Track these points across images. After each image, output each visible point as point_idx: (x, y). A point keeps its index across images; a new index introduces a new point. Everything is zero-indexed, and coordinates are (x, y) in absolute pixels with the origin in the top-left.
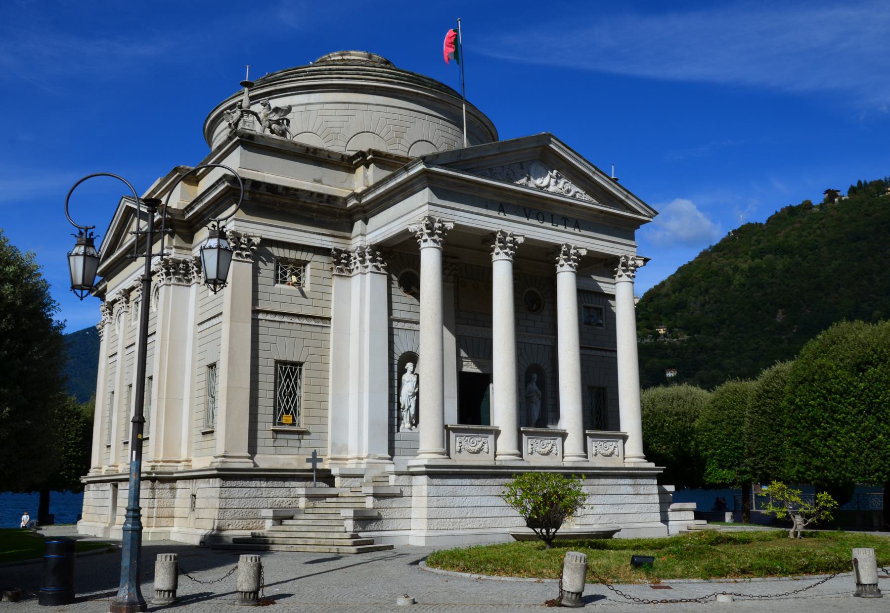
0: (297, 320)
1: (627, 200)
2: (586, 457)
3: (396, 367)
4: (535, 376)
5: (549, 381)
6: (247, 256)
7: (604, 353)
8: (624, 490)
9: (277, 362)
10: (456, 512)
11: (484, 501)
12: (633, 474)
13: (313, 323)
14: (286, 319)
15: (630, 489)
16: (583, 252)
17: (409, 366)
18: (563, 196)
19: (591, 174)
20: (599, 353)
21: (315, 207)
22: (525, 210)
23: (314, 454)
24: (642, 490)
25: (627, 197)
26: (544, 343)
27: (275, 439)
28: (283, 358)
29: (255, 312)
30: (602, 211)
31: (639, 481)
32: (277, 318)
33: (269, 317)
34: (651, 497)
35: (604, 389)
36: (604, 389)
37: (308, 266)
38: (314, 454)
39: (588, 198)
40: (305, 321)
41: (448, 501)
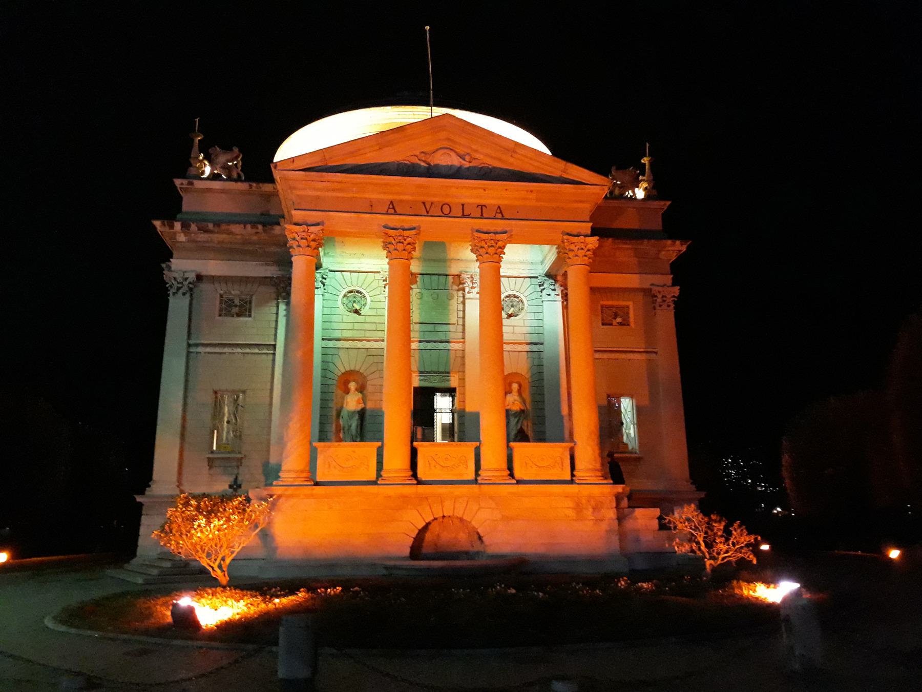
0: (239, 350)
4: (515, 386)
6: (184, 294)
13: (257, 351)
14: (226, 350)
17: (352, 386)
21: (255, 238)
22: (424, 203)
23: (236, 479)
27: (211, 467)
29: (189, 345)
32: (217, 350)
33: (208, 349)
37: (254, 297)
38: (236, 479)
40: (248, 350)
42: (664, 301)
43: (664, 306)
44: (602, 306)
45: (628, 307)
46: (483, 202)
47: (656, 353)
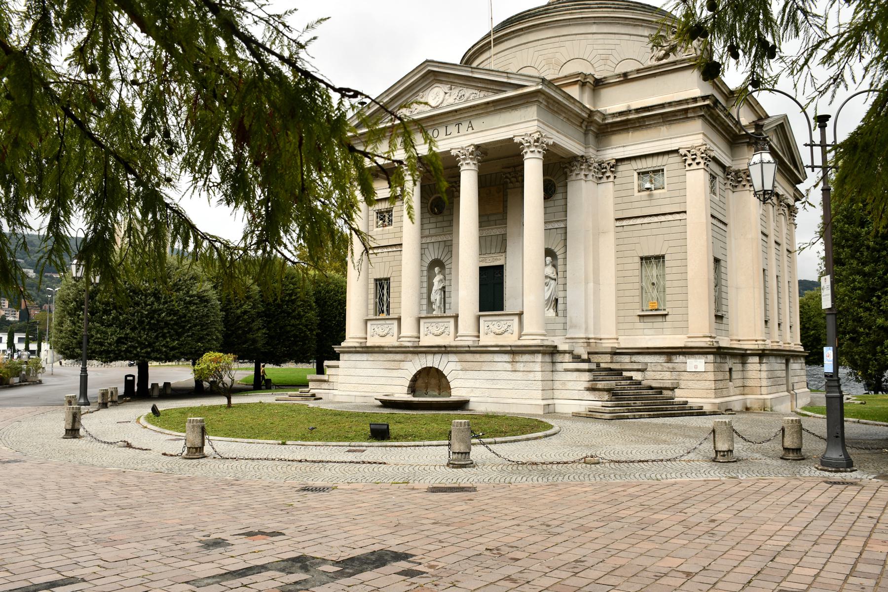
0: (385, 250)
1: (510, 81)
2: (479, 337)
3: (425, 273)
5: (560, 262)
7: (662, 218)
8: (500, 366)
9: (376, 280)
10: (354, 380)
11: (375, 372)
12: (514, 352)
15: (508, 366)
16: (471, 149)
18: (457, 104)
19: (470, 75)
20: (655, 219)
24: (520, 367)
25: (508, 78)
26: (556, 225)
28: (378, 277)
30: (488, 103)
31: (519, 358)
34: (532, 374)
35: (663, 257)
36: (663, 257)
39: (482, 94)
41: (352, 371)
42: (694, 160)
43: (694, 166)
44: (639, 174)
45: (663, 170)
46: (458, 122)
47: (685, 212)
